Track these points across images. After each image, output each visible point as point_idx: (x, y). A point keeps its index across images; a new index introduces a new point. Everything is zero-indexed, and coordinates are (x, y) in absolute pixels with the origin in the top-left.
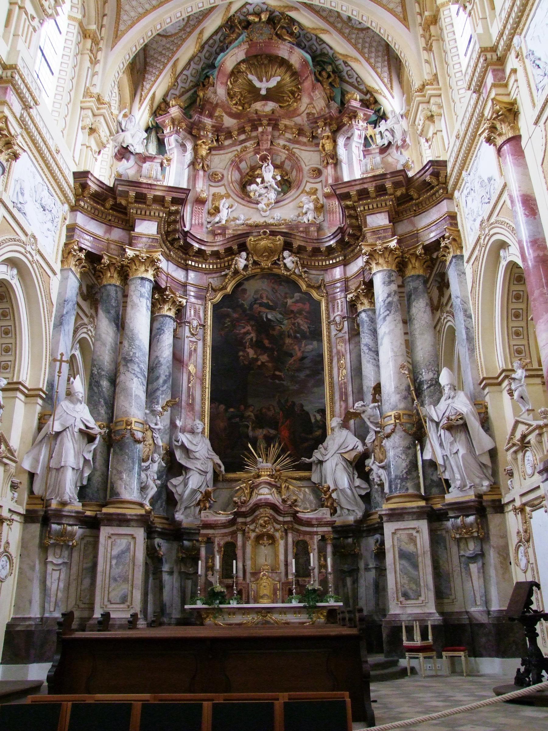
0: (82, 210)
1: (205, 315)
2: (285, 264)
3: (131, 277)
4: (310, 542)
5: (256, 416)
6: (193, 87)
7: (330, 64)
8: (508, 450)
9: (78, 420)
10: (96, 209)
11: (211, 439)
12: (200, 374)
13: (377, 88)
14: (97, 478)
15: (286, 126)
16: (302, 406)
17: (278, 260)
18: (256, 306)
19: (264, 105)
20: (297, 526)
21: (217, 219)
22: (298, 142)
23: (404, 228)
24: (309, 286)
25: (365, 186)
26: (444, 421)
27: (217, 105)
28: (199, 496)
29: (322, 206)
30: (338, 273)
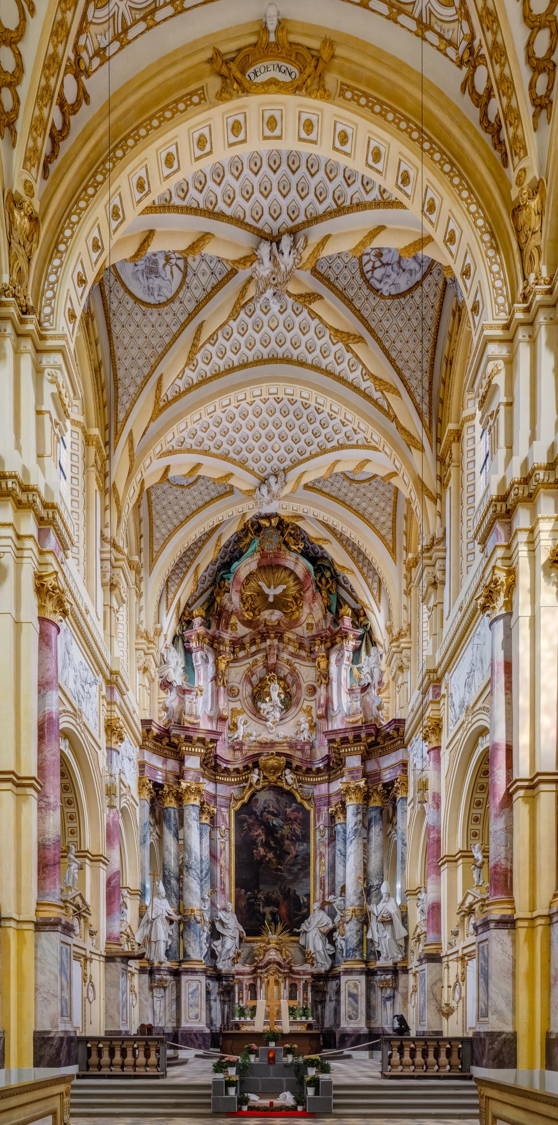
4: (298, 985)
15: (289, 639)
16: (295, 891)
20: (291, 975)
22: (298, 657)
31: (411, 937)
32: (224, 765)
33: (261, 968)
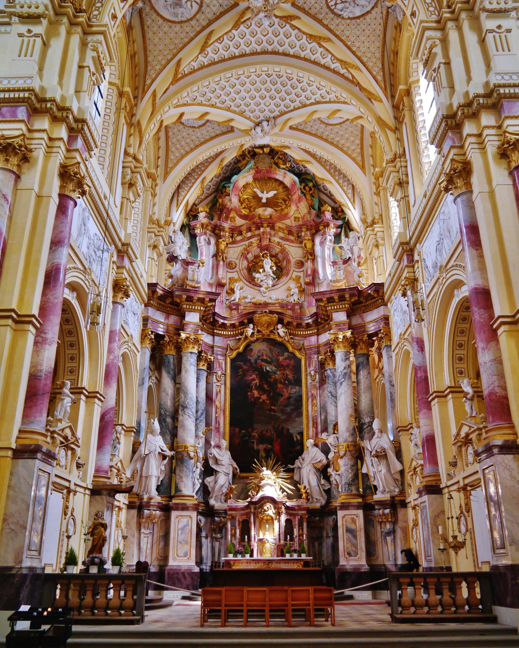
0: (152, 306)
1: (226, 367)
2: (278, 333)
3: (184, 352)
5: (259, 435)
6: (214, 192)
7: (311, 181)
8: (409, 472)
9: (158, 447)
10: (160, 304)
11: (230, 450)
12: (222, 408)
13: (344, 202)
14: (166, 481)
15: (279, 227)
16: (288, 430)
17: (274, 329)
18: (259, 361)
19: (264, 210)
21: (233, 299)
23: (356, 321)
24: (293, 348)
25: (333, 295)
26: (374, 453)
27: (232, 209)
28: (225, 490)
29: (304, 290)
30: (313, 339)
31: (407, 471)
32: (222, 321)
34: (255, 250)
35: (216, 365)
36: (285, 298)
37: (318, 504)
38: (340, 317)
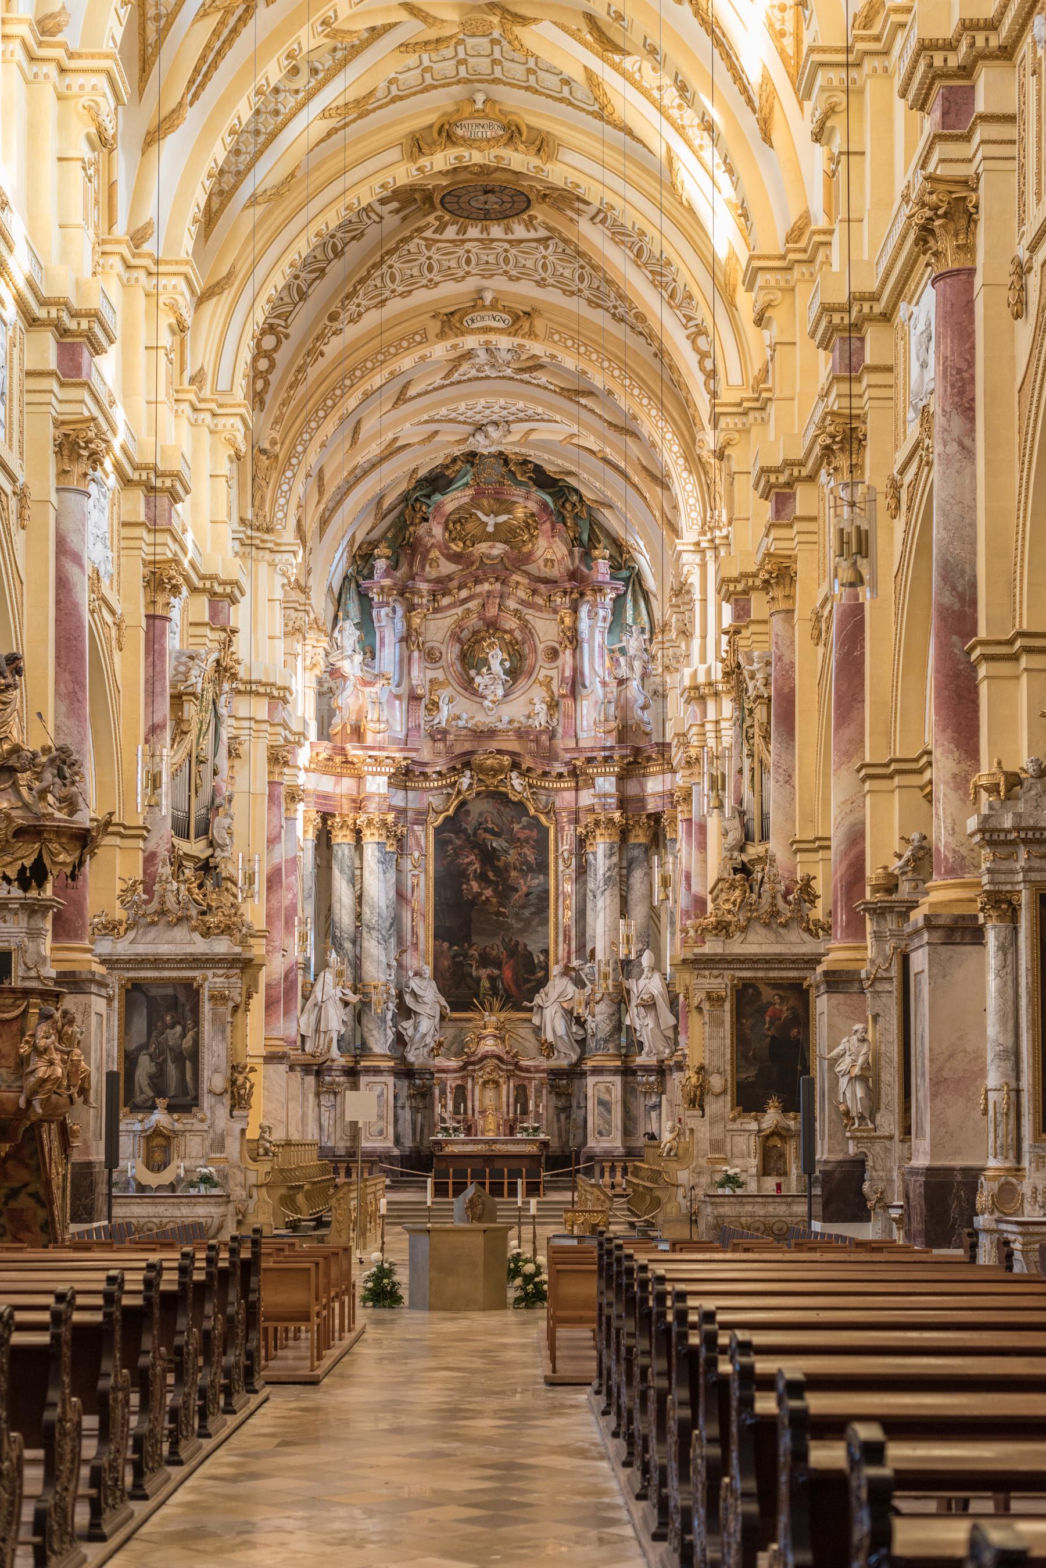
11: (435, 978)
15: (518, 583)
16: (526, 945)
19: (491, 547)
22: (531, 605)
23: (632, 788)
32: (421, 769)
33: (473, 1063)
34: (474, 622)
35: (411, 842)
36: (523, 719)
37: (562, 1061)
38: (607, 784)
